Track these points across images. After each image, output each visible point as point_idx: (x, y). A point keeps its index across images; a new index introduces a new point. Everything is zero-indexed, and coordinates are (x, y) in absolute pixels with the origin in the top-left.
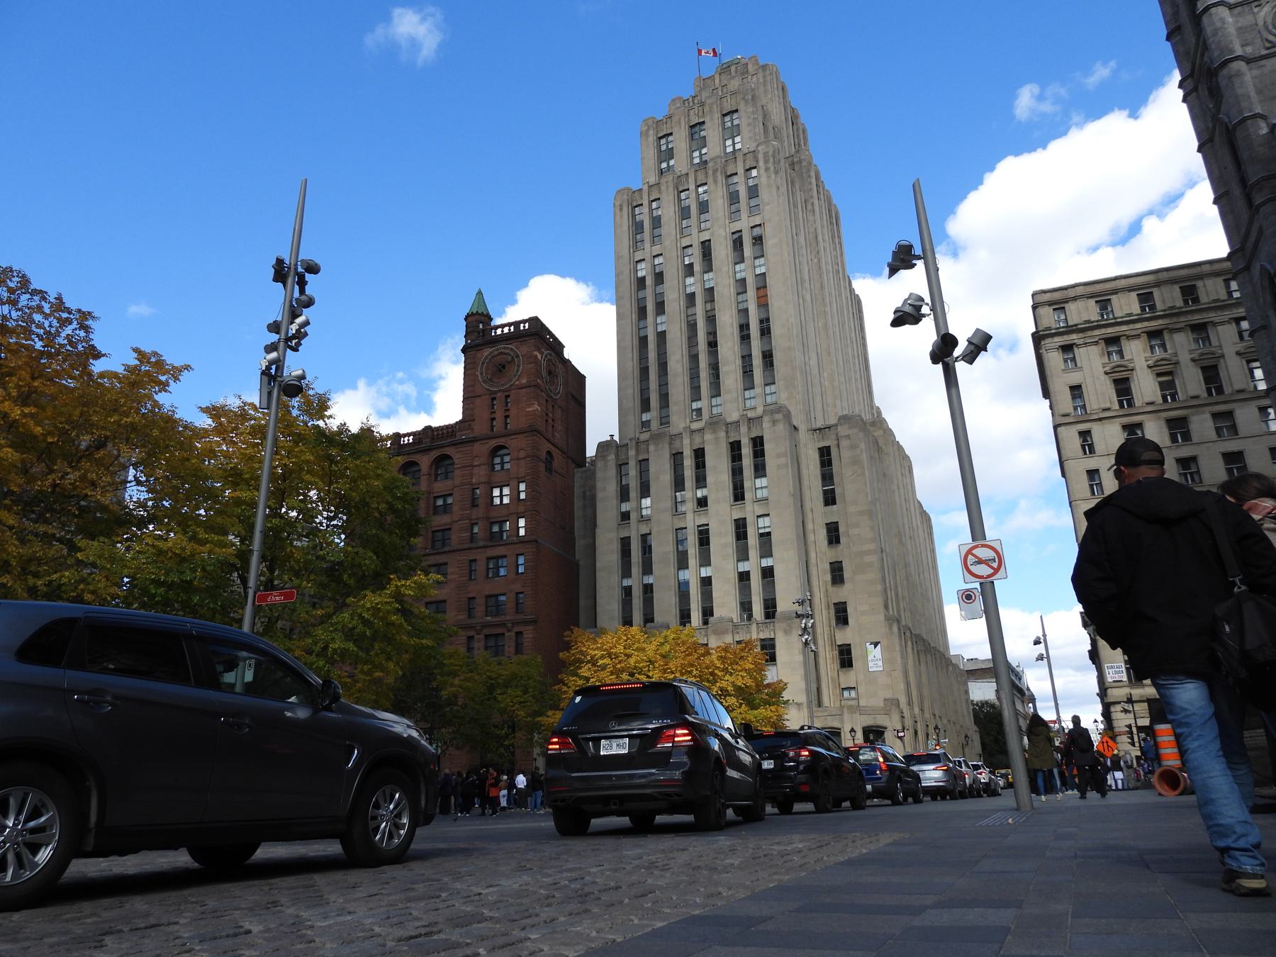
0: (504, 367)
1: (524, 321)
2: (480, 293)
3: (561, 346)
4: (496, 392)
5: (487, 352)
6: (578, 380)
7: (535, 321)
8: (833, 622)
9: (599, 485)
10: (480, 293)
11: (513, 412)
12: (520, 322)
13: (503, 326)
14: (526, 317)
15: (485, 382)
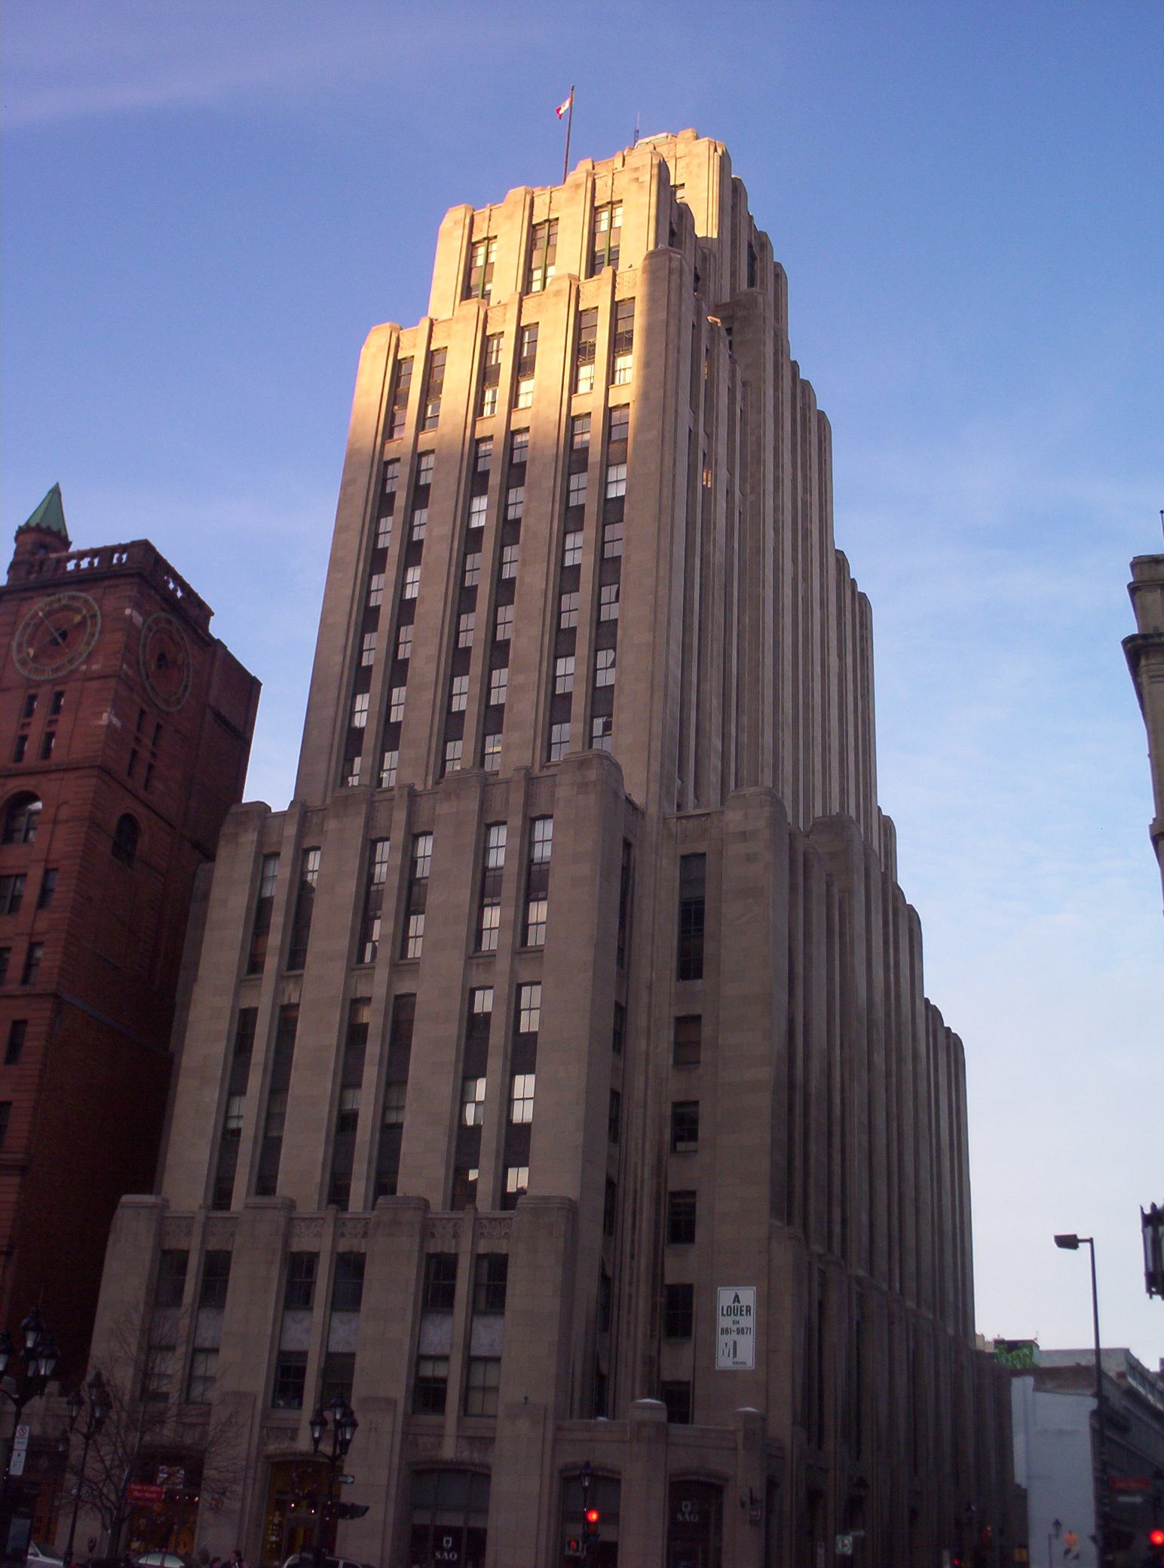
0: (64, 635)
1: (122, 548)
2: (55, 493)
3: (206, 613)
4: (39, 684)
5: (39, 606)
6: (247, 689)
7: (144, 550)
8: (664, 1232)
9: (216, 893)
10: (55, 493)
11: (64, 725)
12: (113, 550)
13: (81, 555)
14: (126, 540)
15: (24, 663)
